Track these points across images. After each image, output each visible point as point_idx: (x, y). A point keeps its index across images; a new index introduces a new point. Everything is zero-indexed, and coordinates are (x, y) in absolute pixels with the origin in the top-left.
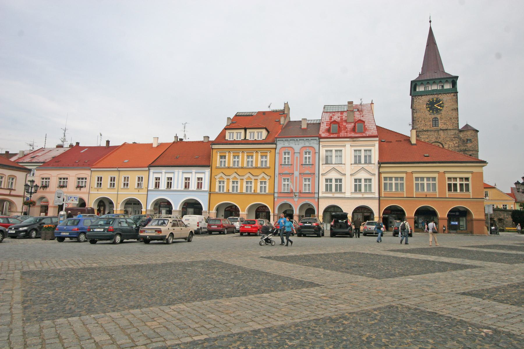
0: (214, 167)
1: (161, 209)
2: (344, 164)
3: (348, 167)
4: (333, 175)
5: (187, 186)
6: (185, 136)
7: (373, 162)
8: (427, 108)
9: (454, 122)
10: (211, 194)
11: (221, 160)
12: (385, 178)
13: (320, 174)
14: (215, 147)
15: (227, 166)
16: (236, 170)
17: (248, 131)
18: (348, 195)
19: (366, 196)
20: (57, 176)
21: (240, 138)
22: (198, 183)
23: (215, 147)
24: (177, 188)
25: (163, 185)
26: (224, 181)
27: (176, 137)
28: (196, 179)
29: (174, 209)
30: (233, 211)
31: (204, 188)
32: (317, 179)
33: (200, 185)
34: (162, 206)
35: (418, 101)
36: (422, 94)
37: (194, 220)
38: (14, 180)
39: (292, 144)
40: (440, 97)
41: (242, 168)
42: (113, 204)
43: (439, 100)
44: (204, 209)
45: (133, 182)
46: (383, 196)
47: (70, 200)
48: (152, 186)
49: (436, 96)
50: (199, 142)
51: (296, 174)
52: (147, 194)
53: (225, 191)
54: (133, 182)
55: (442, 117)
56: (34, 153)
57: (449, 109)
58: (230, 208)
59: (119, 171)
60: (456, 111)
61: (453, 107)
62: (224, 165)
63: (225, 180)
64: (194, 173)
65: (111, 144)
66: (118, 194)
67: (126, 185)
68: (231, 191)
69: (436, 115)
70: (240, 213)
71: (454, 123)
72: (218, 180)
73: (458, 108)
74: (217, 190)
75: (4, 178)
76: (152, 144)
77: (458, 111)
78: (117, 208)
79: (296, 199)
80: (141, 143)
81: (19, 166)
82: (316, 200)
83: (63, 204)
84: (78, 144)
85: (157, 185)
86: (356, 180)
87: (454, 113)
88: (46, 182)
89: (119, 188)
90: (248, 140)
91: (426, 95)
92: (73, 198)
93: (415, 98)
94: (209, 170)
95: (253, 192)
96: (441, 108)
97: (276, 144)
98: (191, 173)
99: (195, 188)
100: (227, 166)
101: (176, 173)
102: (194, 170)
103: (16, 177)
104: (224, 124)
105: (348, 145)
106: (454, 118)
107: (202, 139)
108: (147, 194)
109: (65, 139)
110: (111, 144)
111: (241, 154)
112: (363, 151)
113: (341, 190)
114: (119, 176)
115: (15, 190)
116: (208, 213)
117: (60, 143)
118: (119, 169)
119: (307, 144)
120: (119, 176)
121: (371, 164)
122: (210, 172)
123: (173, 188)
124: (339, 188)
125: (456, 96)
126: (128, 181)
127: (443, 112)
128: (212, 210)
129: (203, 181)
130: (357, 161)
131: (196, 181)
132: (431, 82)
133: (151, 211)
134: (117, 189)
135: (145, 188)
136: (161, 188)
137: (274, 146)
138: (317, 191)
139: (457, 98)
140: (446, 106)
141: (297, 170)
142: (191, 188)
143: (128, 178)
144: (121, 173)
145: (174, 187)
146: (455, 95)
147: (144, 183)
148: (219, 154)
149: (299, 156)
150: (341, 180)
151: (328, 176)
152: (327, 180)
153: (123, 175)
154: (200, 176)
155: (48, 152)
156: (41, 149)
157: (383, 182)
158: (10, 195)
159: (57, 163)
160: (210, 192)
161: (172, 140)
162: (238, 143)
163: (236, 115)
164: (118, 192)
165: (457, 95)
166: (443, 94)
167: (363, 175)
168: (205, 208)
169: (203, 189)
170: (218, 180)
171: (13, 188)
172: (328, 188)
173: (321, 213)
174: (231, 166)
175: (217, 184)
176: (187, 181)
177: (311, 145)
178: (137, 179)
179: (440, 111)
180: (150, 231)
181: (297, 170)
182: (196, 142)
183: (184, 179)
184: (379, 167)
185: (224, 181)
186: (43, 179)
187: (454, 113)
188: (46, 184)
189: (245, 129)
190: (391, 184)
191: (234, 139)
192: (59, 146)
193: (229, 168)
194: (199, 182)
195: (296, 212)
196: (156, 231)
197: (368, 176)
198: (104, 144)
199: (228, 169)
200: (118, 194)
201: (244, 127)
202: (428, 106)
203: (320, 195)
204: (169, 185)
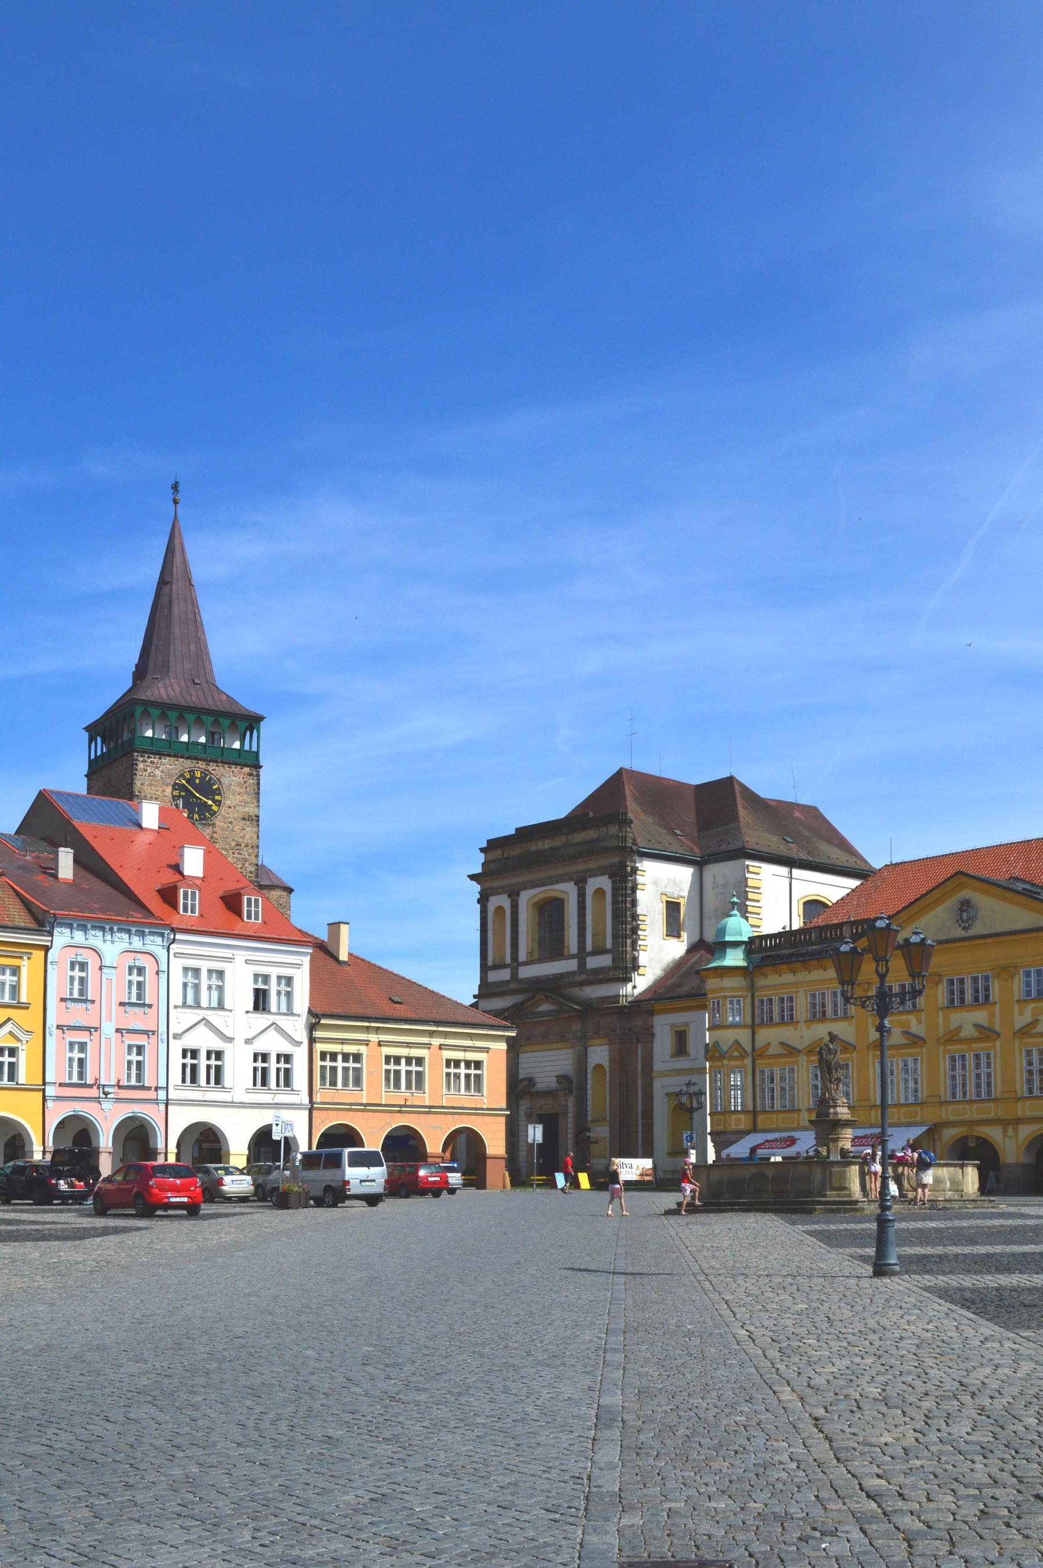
2: (231, 1011)
4: (203, 1040)
8: (174, 797)
9: (247, 856)
18: (240, 1096)
19: (281, 1098)
32: (163, 1047)
35: (149, 770)
36: (157, 749)
40: (216, 770)
43: (211, 778)
46: (319, 1101)
49: (202, 765)
51: (108, 1029)
55: (215, 835)
57: (236, 815)
60: (255, 823)
61: (247, 809)
69: (200, 827)
71: (246, 860)
73: (257, 816)
77: (258, 826)
79: (106, 1105)
82: (162, 1107)
87: (250, 830)
91: (175, 756)
93: (141, 759)
96: (215, 808)
97: (52, 935)
105: (241, 956)
106: (247, 846)
113: (218, 1081)
119: (137, 943)
121: (292, 1014)
124: (217, 1076)
125: (256, 778)
127: (218, 821)
132: (191, 717)
138: (162, 1083)
139: (258, 784)
140: (228, 802)
146: (255, 773)
149: (114, 978)
150: (219, 1055)
151: (190, 1041)
157: (318, 1063)
165: (258, 775)
166: (221, 762)
167: (273, 1044)
172: (191, 1075)
177: (148, 948)
179: (212, 815)
184: (312, 1028)
187: (248, 829)
190: (334, 1070)
202: (176, 793)
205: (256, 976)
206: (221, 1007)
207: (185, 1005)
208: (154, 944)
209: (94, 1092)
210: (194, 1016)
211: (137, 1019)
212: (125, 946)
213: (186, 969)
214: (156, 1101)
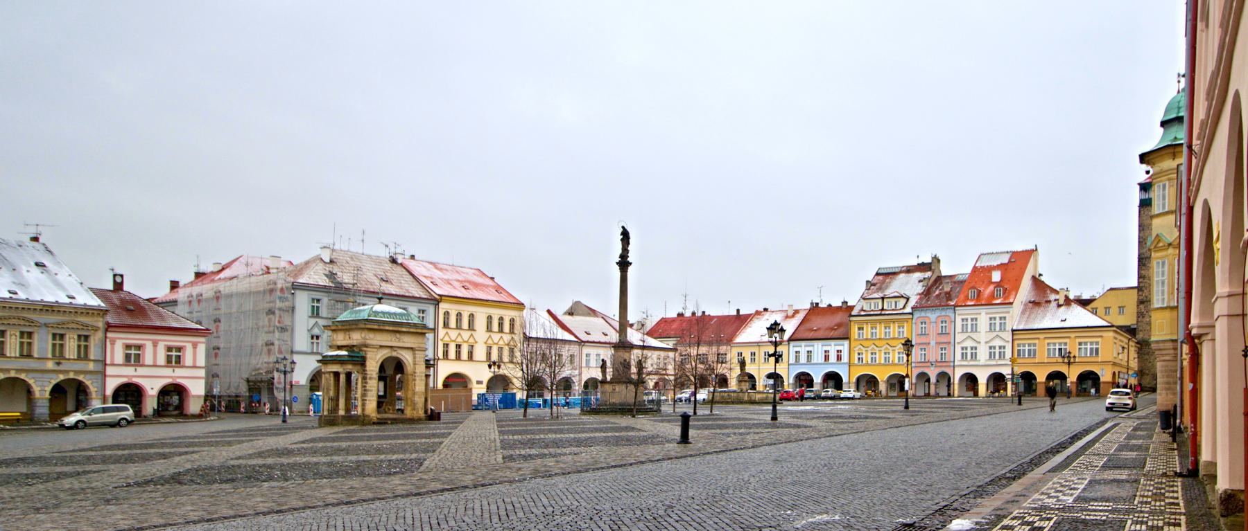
0: (852, 338)
3: (983, 334)
4: (969, 344)
5: (827, 358)
6: (821, 300)
7: (1007, 329)
12: (1019, 345)
13: (956, 341)
15: (865, 337)
17: (885, 300)
18: (982, 362)
19: (999, 363)
22: (838, 355)
24: (818, 360)
25: (803, 359)
27: (812, 304)
28: (836, 352)
29: (815, 381)
32: (952, 348)
33: (839, 358)
39: (929, 314)
41: (880, 339)
44: (844, 381)
48: (792, 360)
51: (933, 343)
59: (759, 346)
64: (833, 345)
65: (741, 313)
68: (870, 362)
74: (856, 362)
79: (932, 368)
82: (952, 368)
84: (704, 312)
85: (797, 358)
86: (990, 348)
95: (891, 362)
101: (816, 346)
102: (833, 343)
107: (840, 305)
110: (742, 313)
112: (998, 319)
117: (681, 310)
119: (943, 313)
124: (974, 356)
130: (992, 328)
137: (910, 316)
141: (933, 340)
144: (761, 348)
145: (814, 360)
148: (856, 326)
151: (964, 345)
152: (962, 349)
157: (1016, 348)
167: (997, 343)
168: (845, 380)
169: (842, 361)
172: (964, 356)
173: (957, 381)
175: (856, 356)
176: (827, 354)
177: (947, 314)
181: (933, 340)
184: (1013, 334)
190: (1024, 350)
193: (867, 339)
195: (933, 380)
197: (1002, 344)
198: (735, 313)
203: (956, 363)
205: (991, 319)
206: (976, 331)
207: (963, 332)
208: (950, 313)
209: (929, 364)
210: (966, 335)
211: (943, 339)
212: (939, 314)
213: (963, 320)
214: (950, 366)
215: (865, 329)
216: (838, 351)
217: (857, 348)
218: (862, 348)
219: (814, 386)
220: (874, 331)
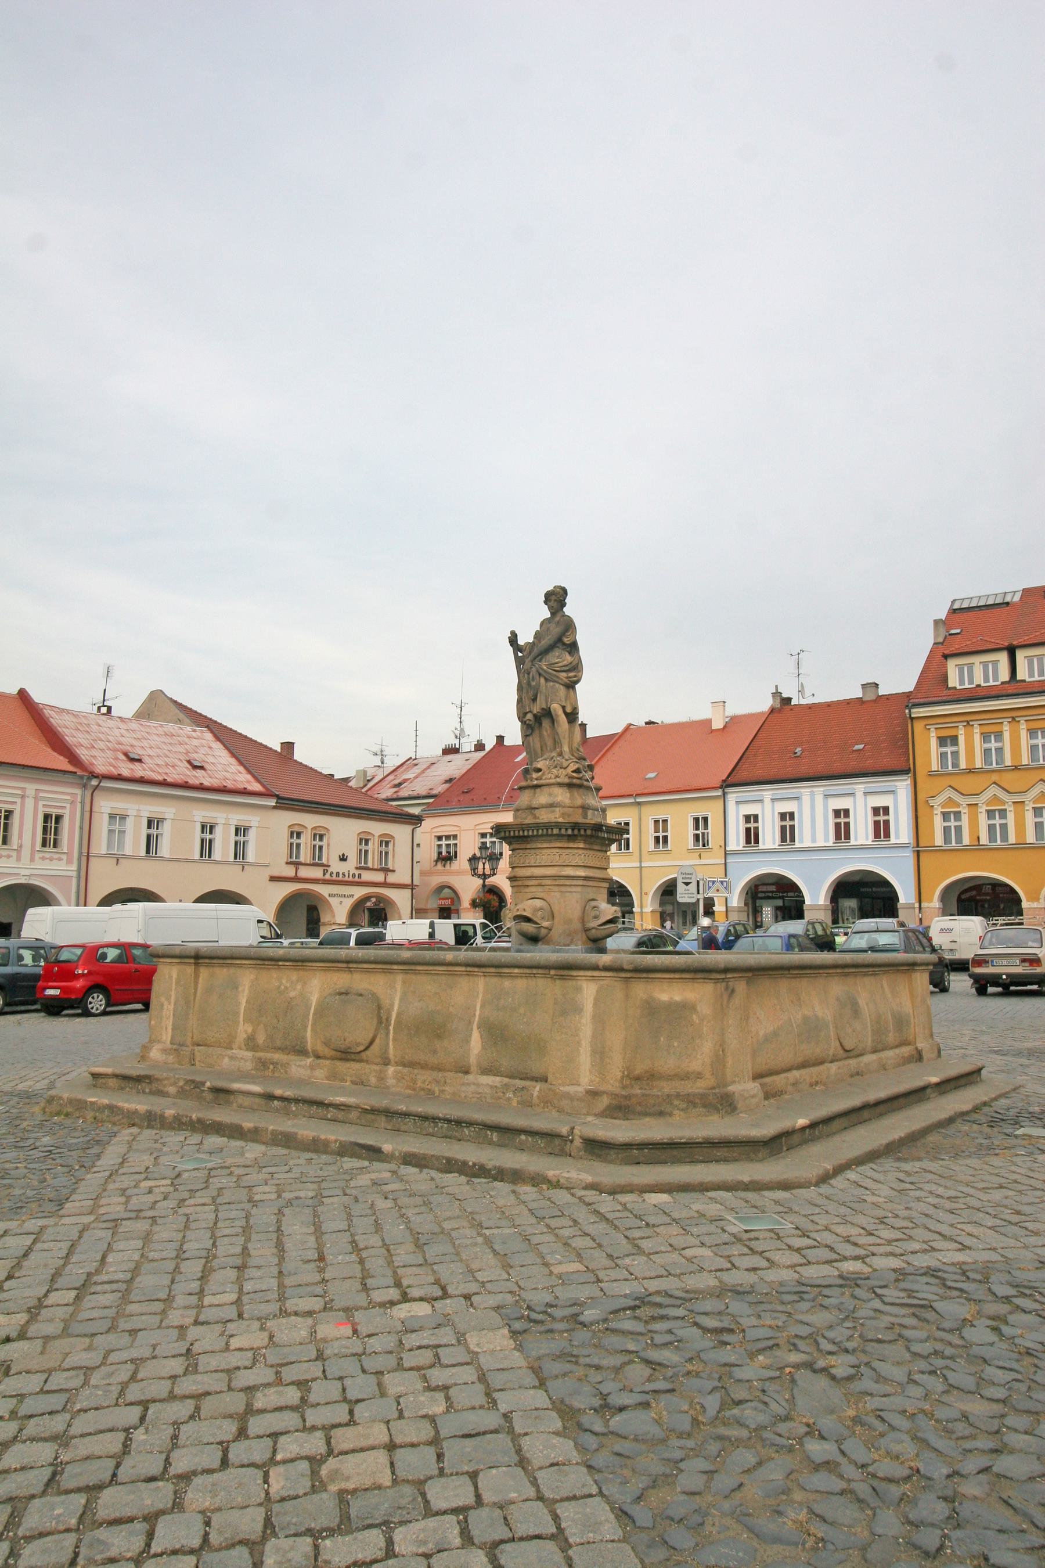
0: (921, 772)
1: (758, 903)
5: (842, 832)
10: (921, 854)
11: (943, 750)
14: (919, 712)
15: (963, 765)
16: (995, 777)
17: (1020, 655)
20: (474, 830)
21: (995, 679)
23: (919, 712)
24: (814, 840)
25: (769, 836)
26: (960, 812)
27: (777, 694)
29: (807, 902)
30: (985, 900)
31: (897, 837)
33: (882, 830)
34: (760, 895)
37: (967, 931)
38: (391, 845)
42: (630, 895)
44: (902, 899)
45: (681, 831)
47: (712, 890)
48: (736, 840)
50: (848, 702)
52: (725, 864)
53: (966, 840)
54: (681, 831)
56: (396, 773)
58: (974, 893)
59: (639, 804)
62: (955, 765)
63: (964, 810)
64: (859, 795)
66: (641, 867)
67: (661, 841)
68: (984, 840)
70: (1025, 904)
72: (938, 810)
74: (939, 840)
75: (370, 843)
76: (708, 722)
78: (642, 907)
80: (669, 720)
81: (390, 810)
83: (698, 900)
84: (500, 739)
85: (752, 837)
88: (448, 846)
89: (644, 852)
90: (1024, 681)
92: (718, 885)
94: (909, 782)
98: (853, 794)
99: (867, 839)
100: (963, 765)
101: (806, 799)
102: (859, 786)
103: (392, 837)
104: (925, 641)
107: (858, 693)
108: (725, 864)
109: (462, 730)
111: (1006, 728)
114: (640, 819)
115: (394, 871)
116: (917, 911)
117: (453, 741)
118: (640, 800)
120: (640, 819)
122: (910, 789)
123: (801, 841)
126: (665, 830)
128: (931, 901)
129: (891, 817)
131: (870, 818)
133: (739, 910)
134: (637, 854)
135: (716, 848)
136: (764, 844)
142: (856, 839)
143: (665, 821)
144: (645, 810)
145: (804, 839)
147: (713, 831)
153: (651, 814)
154: (880, 801)
155: (428, 767)
156: (410, 763)
158: (385, 885)
159: (467, 795)
160: (918, 846)
161: (764, 704)
162: (993, 693)
163: (953, 611)
164: (641, 862)
168: (905, 896)
169: (893, 840)
170: (938, 810)
171: (390, 866)
174: (978, 765)
175: (938, 823)
178: (691, 823)
180: (1005, 962)
182: (839, 703)
183: (831, 815)
185: (960, 812)
186: (440, 838)
188: (449, 853)
189: (1012, 651)
191: (976, 682)
192: (450, 751)
193: (971, 771)
194: (879, 822)
196: (1024, 961)
199: (971, 775)
200: (641, 867)
201: (1006, 644)
204: (787, 834)
215: (961, 740)
216: (876, 811)
217: (942, 798)
218: (956, 797)
219: (806, 913)
220: (993, 745)
